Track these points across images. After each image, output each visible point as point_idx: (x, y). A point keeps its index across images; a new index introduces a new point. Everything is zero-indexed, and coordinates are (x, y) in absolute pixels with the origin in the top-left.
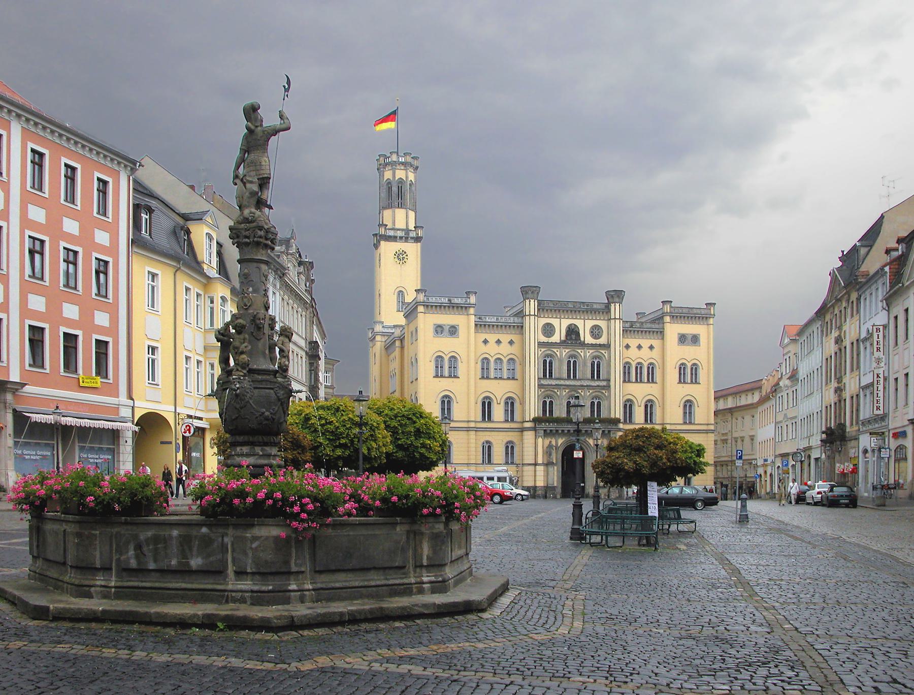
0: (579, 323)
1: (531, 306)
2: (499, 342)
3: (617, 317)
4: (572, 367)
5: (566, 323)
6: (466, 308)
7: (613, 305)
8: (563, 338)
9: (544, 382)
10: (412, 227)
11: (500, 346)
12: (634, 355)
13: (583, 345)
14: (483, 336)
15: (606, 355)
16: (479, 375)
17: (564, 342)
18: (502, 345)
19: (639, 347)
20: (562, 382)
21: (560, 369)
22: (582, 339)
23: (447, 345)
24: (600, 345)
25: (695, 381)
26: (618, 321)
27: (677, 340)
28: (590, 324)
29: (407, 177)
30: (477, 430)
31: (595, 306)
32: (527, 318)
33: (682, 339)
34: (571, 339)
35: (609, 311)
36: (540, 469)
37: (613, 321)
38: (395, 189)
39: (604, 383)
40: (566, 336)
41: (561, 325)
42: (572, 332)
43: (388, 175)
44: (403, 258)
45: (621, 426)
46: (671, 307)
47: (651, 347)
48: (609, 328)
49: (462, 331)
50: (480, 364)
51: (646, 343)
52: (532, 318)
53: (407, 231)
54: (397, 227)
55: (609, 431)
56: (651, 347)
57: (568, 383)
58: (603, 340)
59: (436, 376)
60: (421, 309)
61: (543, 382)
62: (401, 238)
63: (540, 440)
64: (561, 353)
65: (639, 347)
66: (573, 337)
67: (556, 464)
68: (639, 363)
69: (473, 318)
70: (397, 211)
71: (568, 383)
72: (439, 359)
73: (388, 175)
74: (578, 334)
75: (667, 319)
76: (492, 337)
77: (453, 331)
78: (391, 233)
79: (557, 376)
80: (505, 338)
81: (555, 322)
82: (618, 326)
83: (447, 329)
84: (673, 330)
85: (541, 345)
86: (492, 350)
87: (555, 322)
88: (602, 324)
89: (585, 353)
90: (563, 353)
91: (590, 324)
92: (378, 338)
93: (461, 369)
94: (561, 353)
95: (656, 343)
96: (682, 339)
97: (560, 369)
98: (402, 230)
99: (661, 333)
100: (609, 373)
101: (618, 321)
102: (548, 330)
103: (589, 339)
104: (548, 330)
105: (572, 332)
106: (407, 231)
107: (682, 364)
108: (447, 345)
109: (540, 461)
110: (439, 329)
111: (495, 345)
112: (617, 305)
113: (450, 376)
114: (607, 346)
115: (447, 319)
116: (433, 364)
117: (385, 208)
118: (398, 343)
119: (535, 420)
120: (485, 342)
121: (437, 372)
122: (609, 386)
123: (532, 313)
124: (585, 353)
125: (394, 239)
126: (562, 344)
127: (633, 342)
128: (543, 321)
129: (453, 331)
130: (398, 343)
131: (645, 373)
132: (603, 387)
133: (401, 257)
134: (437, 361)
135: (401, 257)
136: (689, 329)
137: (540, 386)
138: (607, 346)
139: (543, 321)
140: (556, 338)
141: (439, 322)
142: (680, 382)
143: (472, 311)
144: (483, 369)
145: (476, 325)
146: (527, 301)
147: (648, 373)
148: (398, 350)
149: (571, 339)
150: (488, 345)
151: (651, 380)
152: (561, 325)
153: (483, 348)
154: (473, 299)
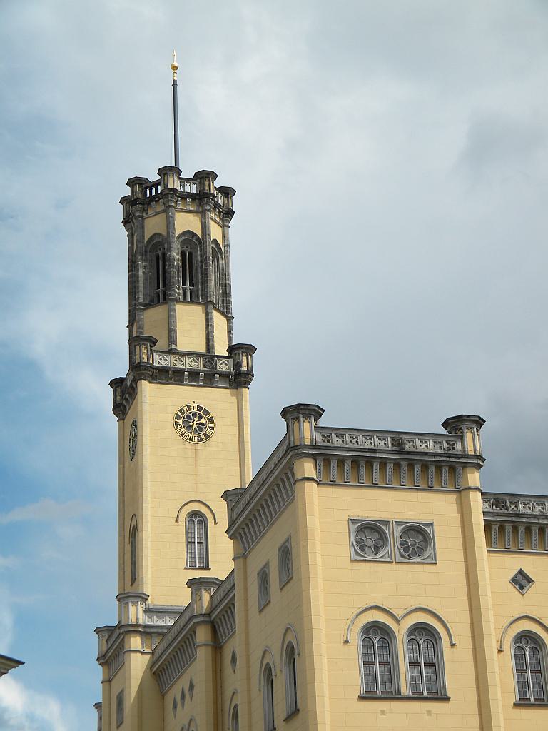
10: (221, 348)
14: (513, 563)
16: (514, 697)
23: (399, 588)
29: (204, 227)
38: (175, 255)
43: (153, 225)
44: (201, 427)
50: (510, 652)
53: (209, 356)
54: (180, 348)
60: (308, 468)
62: (194, 375)
69: (477, 505)
70: (181, 309)
72: (376, 634)
73: (153, 225)
77: (417, 541)
78: (169, 362)
83: (395, 534)
92: (136, 642)
98: (196, 355)
106: (209, 356)
108: (399, 588)
110: (369, 536)
113: (416, 697)
116: (355, 652)
117: (147, 306)
118: (203, 635)
121: (369, 679)
125: (173, 376)
129: (417, 541)
134: (367, 642)
143: (474, 478)
144: (521, 671)
145: (488, 526)
148: (202, 657)
153: (518, 604)
154: (471, 442)
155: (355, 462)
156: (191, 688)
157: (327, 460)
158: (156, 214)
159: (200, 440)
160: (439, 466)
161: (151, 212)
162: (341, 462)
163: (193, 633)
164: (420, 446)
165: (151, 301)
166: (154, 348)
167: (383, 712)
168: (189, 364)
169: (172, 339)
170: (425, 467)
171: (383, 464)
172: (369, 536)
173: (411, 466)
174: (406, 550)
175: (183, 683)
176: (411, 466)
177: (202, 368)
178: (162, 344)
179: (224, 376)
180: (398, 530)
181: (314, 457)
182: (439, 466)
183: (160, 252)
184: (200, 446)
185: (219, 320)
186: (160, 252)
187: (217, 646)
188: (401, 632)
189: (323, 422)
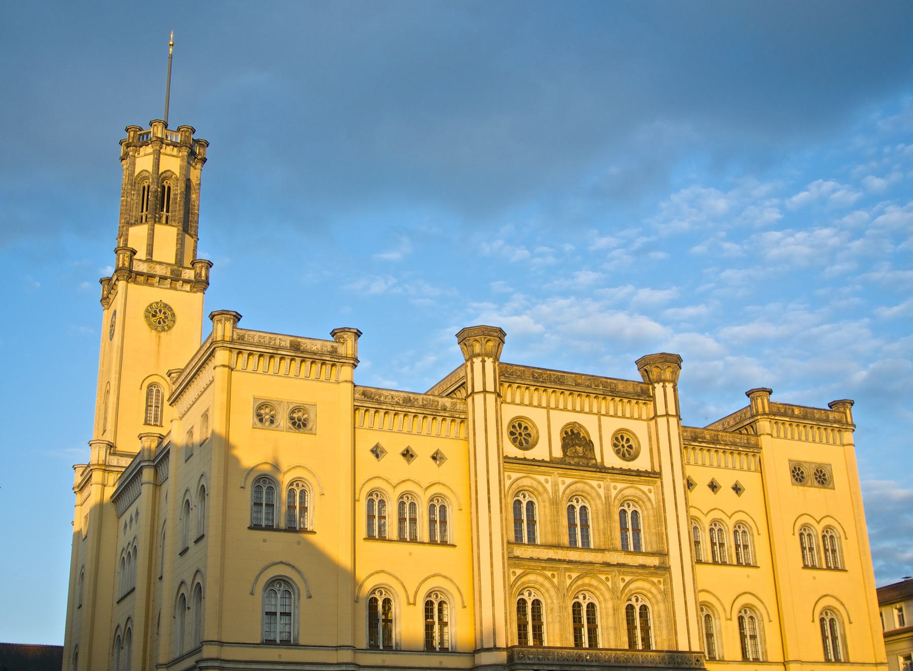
0: (589, 423)
1: (483, 374)
2: (408, 454)
3: (672, 411)
4: (577, 521)
5: (561, 420)
7: (659, 387)
8: (558, 453)
9: (519, 551)
10: (187, 262)
13: (602, 469)
15: (652, 496)
18: (415, 462)
21: (549, 524)
22: (599, 460)
24: (638, 473)
27: (788, 475)
28: (611, 426)
32: (479, 398)
35: (652, 398)
37: (662, 421)
39: (655, 561)
40: (565, 447)
46: (770, 403)
47: (737, 489)
48: (654, 437)
57: (573, 555)
58: (642, 463)
59: (255, 527)
61: (519, 551)
62: (163, 278)
64: (555, 485)
65: (713, 486)
71: (573, 555)
74: (589, 445)
75: (764, 425)
79: (550, 540)
82: (669, 433)
87: (537, 417)
88: (639, 429)
94: (555, 485)
96: (798, 475)
97: (549, 524)
100: (662, 537)
101: (674, 421)
103: (612, 460)
107: (805, 526)
112: (669, 386)
114: (654, 475)
122: (664, 568)
123: (490, 387)
124: (607, 489)
128: (510, 413)
130: (147, 475)
131: (728, 547)
133: (160, 318)
134: (257, 489)
135: (160, 318)
136: (812, 450)
137: (514, 560)
138: (654, 475)
140: (539, 452)
141: (267, 394)
142: (806, 567)
146: (477, 362)
147: (728, 547)
148: (146, 491)
150: (384, 459)
156: (137, 514)
158: (145, 155)
159: (164, 330)
161: (142, 153)
163: (140, 472)
165: (136, 221)
166: (135, 257)
167: (265, 541)
168: (160, 270)
169: (150, 252)
174: (294, 424)
175: (132, 510)
177: (169, 275)
178: (141, 254)
179: (186, 282)
183: (146, 185)
184: (163, 334)
185: (189, 241)
186: (146, 185)
187: (157, 485)
189: (240, 325)
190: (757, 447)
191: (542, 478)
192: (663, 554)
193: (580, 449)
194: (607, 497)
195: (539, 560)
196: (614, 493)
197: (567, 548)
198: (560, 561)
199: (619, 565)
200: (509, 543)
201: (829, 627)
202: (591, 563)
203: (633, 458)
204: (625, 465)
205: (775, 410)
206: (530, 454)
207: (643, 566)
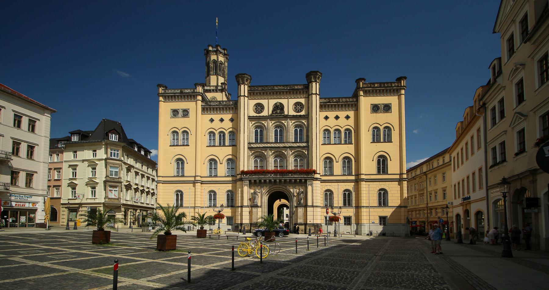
0: (284, 101)
5: (273, 102)
6: (194, 96)
8: (270, 112)
11: (223, 122)
12: (332, 123)
13: (287, 117)
14: (210, 117)
17: (271, 115)
19: (337, 118)
20: (269, 145)
23: (180, 123)
25: (388, 139)
26: (314, 96)
30: (202, 183)
31: (296, 87)
33: (375, 108)
34: (276, 113)
36: (246, 211)
37: (310, 97)
39: (304, 145)
40: (273, 112)
41: (269, 104)
42: (279, 108)
45: (317, 176)
46: (363, 84)
49: (192, 113)
51: (342, 114)
52: (246, 99)
55: (306, 181)
56: (348, 117)
60: (161, 99)
61: (252, 146)
63: (246, 189)
66: (279, 111)
67: (261, 206)
68: (336, 130)
69: (200, 103)
71: (273, 145)
76: (216, 117)
80: (227, 117)
81: (264, 102)
82: (316, 100)
84: (366, 102)
85: (251, 118)
86: (217, 125)
87: (264, 102)
89: (288, 123)
90: (270, 125)
91: (293, 101)
93: (191, 138)
95: (351, 114)
99: (355, 106)
100: (308, 136)
102: (259, 108)
103: (292, 113)
104: (259, 108)
105: (279, 108)
109: (245, 204)
110: (175, 113)
111: (219, 122)
113: (183, 145)
115: (180, 105)
119: (243, 173)
120: (212, 120)
124: (288, 123)
126: (270, 118)
127: (331, 114)
129: (186, 113)
132: (304, 147)
137: (250, 148)
138: (307, 117)
139: (253, 102)
140: (265, 113)
142: (373, 142)
149: (276, 113)
150: (214, 122)
151: (348, 142)
152: (269, 104)
155: (172, 96)
157: (165, 97)
160: (191, 96)
162: (168, 97)
164: (186, 91)
170: (188, 96)
171: (178, 96)
172: (175, 113)
173: (184, 96)
176: (184, 96)
180: (181, 111)
181: (162, 96)
182: (191, 96)
188: (180, 132)
190: (357, 101)
191: (263, 122)
192: (307, 142)
193: (279, 111)
194: (287, 125)
195: (260, 148)
196: (291, 124)
197: (272, 143)
198: (267, 147)
199: (290, 147)
200: (249, 143)
201: (382, 163)
202: (279, 147)
203: (301, 111)
204: (295, 114)
205: (365, 86)
206: (261, 115)
207: (299, 147)
